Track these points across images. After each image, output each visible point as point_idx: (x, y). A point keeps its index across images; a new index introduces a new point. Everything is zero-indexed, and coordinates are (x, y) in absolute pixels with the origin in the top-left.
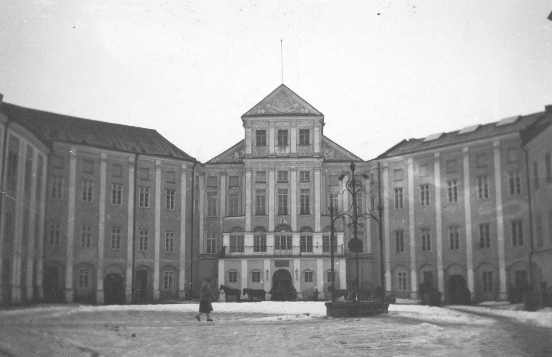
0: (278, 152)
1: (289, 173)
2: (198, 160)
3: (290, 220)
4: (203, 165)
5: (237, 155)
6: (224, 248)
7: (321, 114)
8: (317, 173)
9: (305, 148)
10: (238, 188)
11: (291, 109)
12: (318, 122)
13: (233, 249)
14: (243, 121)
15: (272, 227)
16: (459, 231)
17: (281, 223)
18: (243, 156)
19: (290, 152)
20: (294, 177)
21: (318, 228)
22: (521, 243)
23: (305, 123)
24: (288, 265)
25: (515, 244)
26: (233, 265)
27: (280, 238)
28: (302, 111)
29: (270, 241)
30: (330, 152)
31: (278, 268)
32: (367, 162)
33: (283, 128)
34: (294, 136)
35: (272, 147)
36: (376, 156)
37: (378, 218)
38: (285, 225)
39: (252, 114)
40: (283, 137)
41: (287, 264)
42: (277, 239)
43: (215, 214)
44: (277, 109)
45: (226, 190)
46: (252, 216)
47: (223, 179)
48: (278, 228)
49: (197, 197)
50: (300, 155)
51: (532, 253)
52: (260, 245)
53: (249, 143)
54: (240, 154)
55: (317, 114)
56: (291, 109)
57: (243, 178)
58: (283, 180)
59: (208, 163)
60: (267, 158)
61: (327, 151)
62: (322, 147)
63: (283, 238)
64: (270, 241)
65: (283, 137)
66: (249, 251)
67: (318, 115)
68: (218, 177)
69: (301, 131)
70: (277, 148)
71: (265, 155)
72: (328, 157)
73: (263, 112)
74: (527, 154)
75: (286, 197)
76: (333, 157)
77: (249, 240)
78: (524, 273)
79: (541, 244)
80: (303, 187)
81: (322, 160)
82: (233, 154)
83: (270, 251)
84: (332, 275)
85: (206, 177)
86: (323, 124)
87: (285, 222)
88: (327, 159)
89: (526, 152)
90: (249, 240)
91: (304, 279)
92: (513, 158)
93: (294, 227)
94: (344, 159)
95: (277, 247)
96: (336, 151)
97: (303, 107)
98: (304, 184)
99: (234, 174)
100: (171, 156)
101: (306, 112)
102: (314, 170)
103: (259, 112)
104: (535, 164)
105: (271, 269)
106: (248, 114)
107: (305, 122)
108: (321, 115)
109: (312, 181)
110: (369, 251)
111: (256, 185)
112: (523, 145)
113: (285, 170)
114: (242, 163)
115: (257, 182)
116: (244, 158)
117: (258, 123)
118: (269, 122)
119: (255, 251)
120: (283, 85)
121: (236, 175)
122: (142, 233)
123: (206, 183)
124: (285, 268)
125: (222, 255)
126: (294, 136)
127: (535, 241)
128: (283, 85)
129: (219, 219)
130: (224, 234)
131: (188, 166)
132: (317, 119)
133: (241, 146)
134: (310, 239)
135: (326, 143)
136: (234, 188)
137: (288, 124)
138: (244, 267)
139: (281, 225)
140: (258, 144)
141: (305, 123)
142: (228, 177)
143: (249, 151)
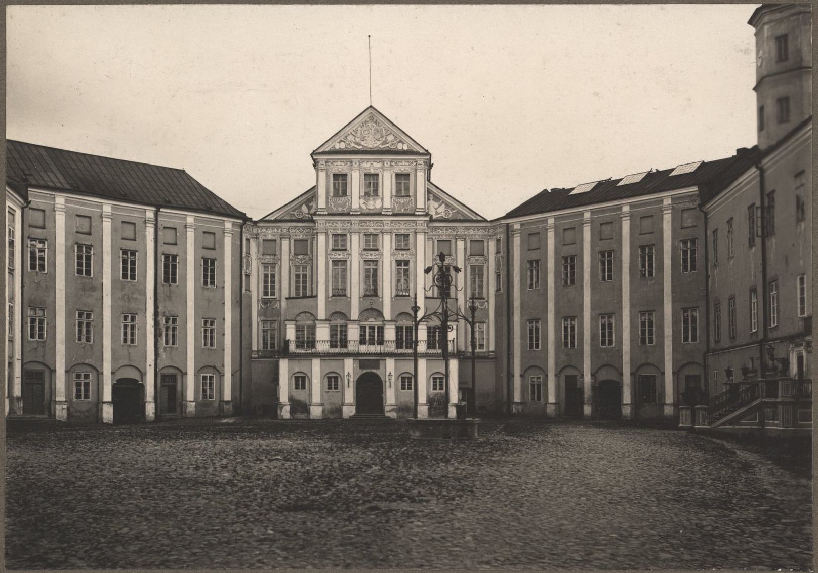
0: (364, 207)
1: (380, 236)
2: (249, 216)
4: (255, 223)
5: (304, 209)
6: (287, 342)
7: (427, 151)
8: (420, 238)
9: (402, 201)
10: (307, 257)
11: (382, 144)
13: (299, 343)
14: (314, 160)
15: (355, 314)
16: (575, 323)
18: (312, 211)
19: (382, 207)
20: (387, 244)
22: (694, 338)
23: (403, 166)
24: (378, 367)
25: (686, 339)
26: (298, 366)
28: (400, 147)
29: (353, 333)
30: (439, 206)
31: (365, 371)
32: (492, 221)
33: (372, 172)
34: (387, 183)
36: (504, 214)
37: (470, 320)
39: (327, 150)
41: (376, 364)
42: (363, 329)
43: (273, 294)
44: (363, 143)
45: (290, 260)
46: (327, 297)
47: (285, 243)
49: (247, 268)
50: (396, 212)
51: (708, 351)
52: (339, 338)
53: (322, 192)
54: (309, 208)
55: (422, 151)
56: (382, 144)
57: (315, 242)
59: (262, 220)
60: (348, 214)
61: (436, 205)
62: (429, 200)
63: (372, 328)
64: (353, 333)
66: (322, 347)
68: (278, 241)
69: (398, 176)
70: (362, 201)
71: (345, 210)
72: (437, 213)
73: (342, 146)
74: (706, 219)
75: (375, 271)
76: (443, 214)
77: (323, 333)
78: (697, 378)
79: (717, 342)
80: (400, 257)
81: (427, 218)
82: (300, 207)
83: (352, 348)
84: (440, 381)
85: (261, 241)
86: (431, 166)
88: (434, 217)
89: (706, 214)
90: (323, 333)
92: (689, 222)
93: (387, 315)
94: (460, 217)
95: (362, 341)
96: (448, 205)
97: (400, 141)
98: (401, 252)
99: (301, 237)
100: (208, 211)
101: (405, 148)
102: (416, 233)
103: (337, 147)
104: (715, 231)
106: (321, 150)
107: (404, 163)
108: (427, 153)
110: (492, 348)
112: (701, 206)
113: (374, 232)
114: (313, 221)
115: (333, 250)
116: (315, 214)
118: (351, 162)
119: (331, 346)
120: (371, 107)
121: (305, 238)
122: (167, 320)
124: (374, 371)
125: (284, 352)
126: (387, 183)
127: (712, 338)
128: (371, 107)
129: (280, 301)
130: (287, 323)
131: (234, 224)
132: (421, 160)
133: (310, 196)
135: (433, 193)
136: (301, 257)
137: (380, 165)
138: (316, 369)
140: (336, 194)
141: (403, 166)
142: (293, 242)
143: (322, 203)
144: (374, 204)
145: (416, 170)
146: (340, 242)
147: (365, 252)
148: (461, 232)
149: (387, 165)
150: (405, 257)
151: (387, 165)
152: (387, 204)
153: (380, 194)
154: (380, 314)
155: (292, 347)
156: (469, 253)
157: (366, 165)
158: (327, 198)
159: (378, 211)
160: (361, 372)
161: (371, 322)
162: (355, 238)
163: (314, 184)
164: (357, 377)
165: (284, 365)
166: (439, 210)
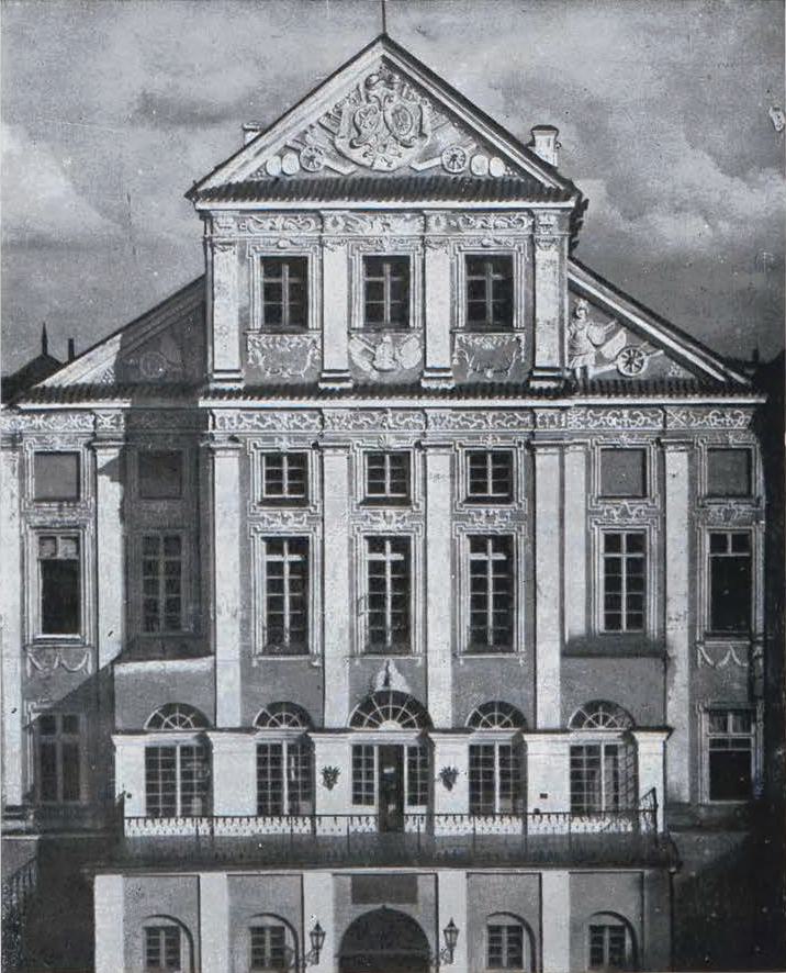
0: (365, 365)
1: (416, 456)
3: (421, 677)
9: (488, 342)
12: (553, 220)
15: (338, 710)
17: (379, 687)
20: (439, 484)
21: (549, 704)
23: (496, 231)
26: (163, 891)
27: (376, 749)
30: (609, 336)
33: (388, 250)
35: (337, 331)
38: (400, 697)
39: (240, 178)
40: (388, 293)
44: (356, 155)
46: (246, 655)
48: (370, 706)
50: (470, 377)
52: (287, 778)
53: (225, 315)
58: (388, 494)
65: (388, 293)
67: (555, 195)
69: (475, 263)
70: (358, 346)
71: (304, 375)
73: (291, 165)
75: (402, 568)
80: (480, 526)
85: (30, 455)
87: (399, 684)
91: (483, 957)
93: (440, 709)
101: (498, 169)
102: (531, 448)
105: (338, 919)
106: (217, 181)
109: (523, 499)
111: (265, 512)
115: (265, 502)
117: (267, 224)
118: (322, 219)
123: (31, 482)
125: (114, 853)
126: (440, 292)
132: (550, 214)
134: (515, 756)
139: (383, 697)
141: (496, 231)
143: (225, 354)
144: (397, 356)
145: (533, 242)
146: (288, 477)
147: (365, 511)
148: (677, 420)
149: (437, 229)
150: (499, 526)
151: (437, 229)
152: (440, 356)
153: (415, 322)
154: (414, 710)
155: (139, 827)
156: (704, 489)
157: (372, 228)
158: (244, 335)
159: (410, 379)
160: (356, 911)
161: (391, 731)
162: (336, 463)
163: (203, 272)
164: (344, 927)
165: (110, 893)
166: (610, 350)
